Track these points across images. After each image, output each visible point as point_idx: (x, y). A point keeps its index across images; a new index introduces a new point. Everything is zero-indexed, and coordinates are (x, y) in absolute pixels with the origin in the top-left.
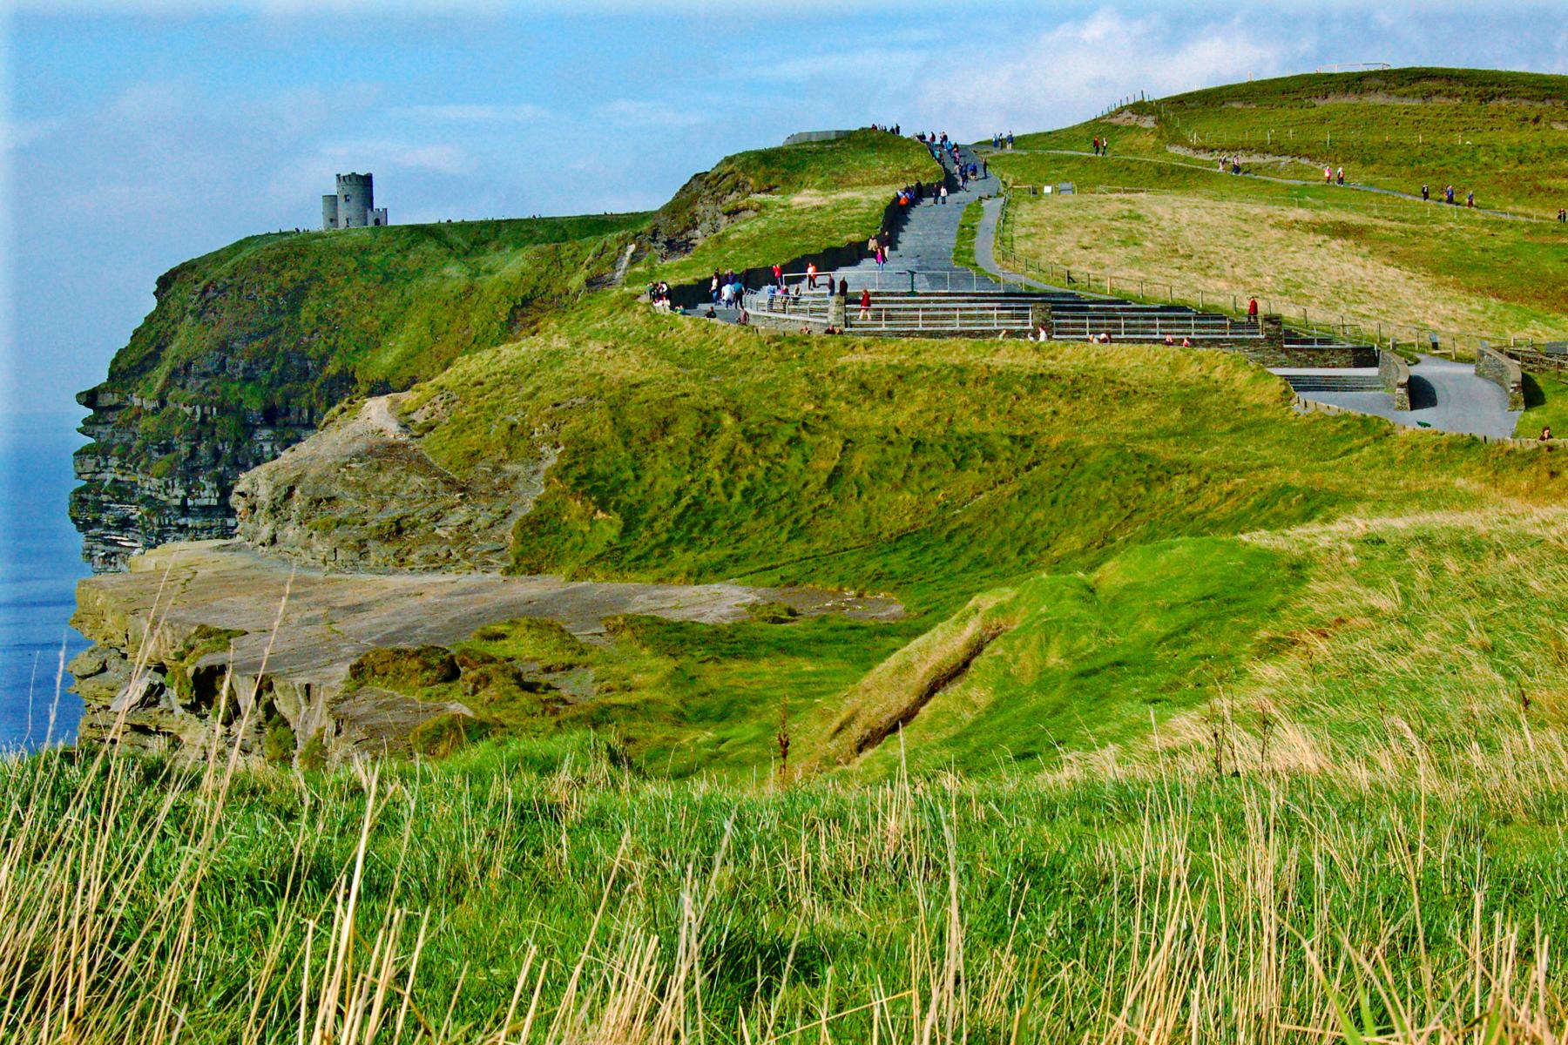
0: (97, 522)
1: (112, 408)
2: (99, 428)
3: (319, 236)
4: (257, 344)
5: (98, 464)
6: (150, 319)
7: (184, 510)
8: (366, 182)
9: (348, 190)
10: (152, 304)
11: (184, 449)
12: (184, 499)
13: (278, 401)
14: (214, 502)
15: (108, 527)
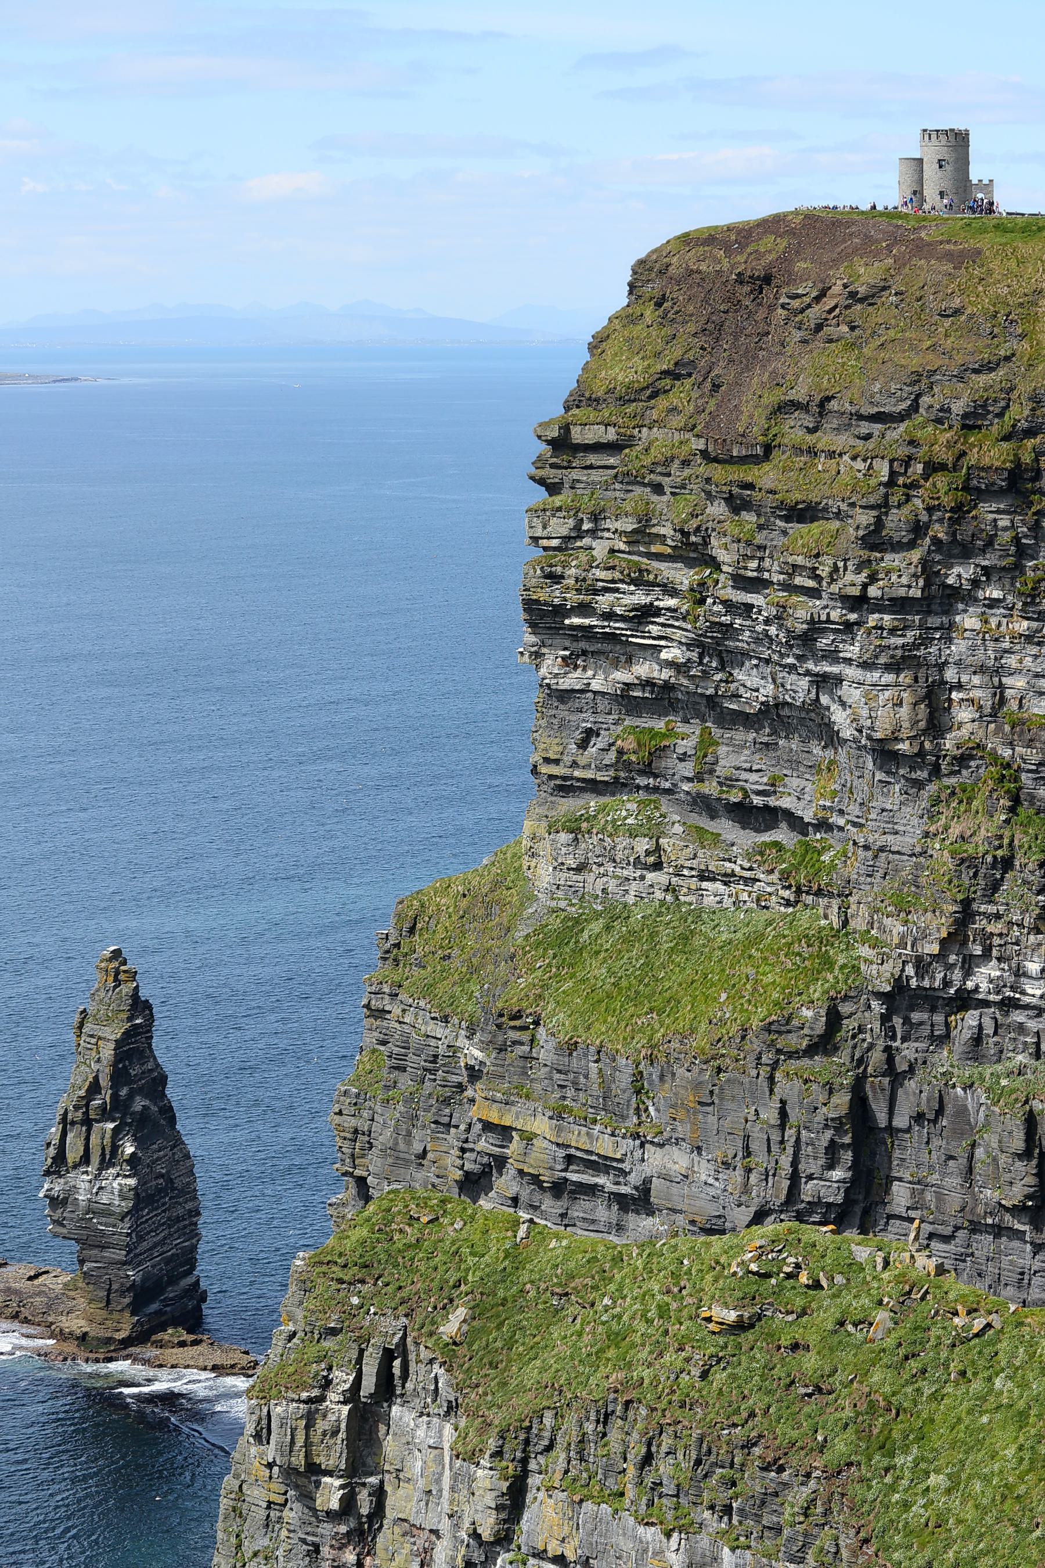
0: (584, 609)
1: (597, 447)
2: (575, 474)
3: (892, 215)
4: (982, 379)
5: (578, 527)
6: (627, 318)
7: (859, 602)
8: (959, 140)
9: (944, 153)
10: (620, 299)
11: (865, 518)
12: (865, 586)
13: (1027, 458)
14: (916, 593)
15: (609, 616)
